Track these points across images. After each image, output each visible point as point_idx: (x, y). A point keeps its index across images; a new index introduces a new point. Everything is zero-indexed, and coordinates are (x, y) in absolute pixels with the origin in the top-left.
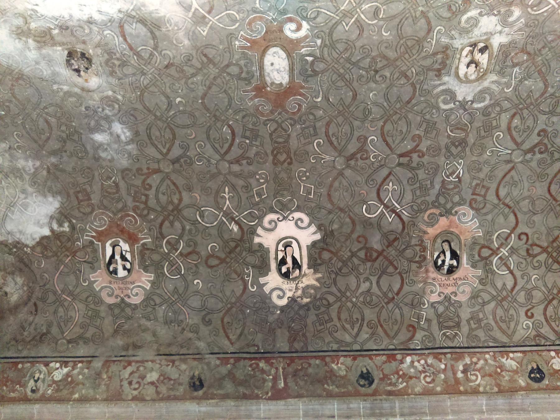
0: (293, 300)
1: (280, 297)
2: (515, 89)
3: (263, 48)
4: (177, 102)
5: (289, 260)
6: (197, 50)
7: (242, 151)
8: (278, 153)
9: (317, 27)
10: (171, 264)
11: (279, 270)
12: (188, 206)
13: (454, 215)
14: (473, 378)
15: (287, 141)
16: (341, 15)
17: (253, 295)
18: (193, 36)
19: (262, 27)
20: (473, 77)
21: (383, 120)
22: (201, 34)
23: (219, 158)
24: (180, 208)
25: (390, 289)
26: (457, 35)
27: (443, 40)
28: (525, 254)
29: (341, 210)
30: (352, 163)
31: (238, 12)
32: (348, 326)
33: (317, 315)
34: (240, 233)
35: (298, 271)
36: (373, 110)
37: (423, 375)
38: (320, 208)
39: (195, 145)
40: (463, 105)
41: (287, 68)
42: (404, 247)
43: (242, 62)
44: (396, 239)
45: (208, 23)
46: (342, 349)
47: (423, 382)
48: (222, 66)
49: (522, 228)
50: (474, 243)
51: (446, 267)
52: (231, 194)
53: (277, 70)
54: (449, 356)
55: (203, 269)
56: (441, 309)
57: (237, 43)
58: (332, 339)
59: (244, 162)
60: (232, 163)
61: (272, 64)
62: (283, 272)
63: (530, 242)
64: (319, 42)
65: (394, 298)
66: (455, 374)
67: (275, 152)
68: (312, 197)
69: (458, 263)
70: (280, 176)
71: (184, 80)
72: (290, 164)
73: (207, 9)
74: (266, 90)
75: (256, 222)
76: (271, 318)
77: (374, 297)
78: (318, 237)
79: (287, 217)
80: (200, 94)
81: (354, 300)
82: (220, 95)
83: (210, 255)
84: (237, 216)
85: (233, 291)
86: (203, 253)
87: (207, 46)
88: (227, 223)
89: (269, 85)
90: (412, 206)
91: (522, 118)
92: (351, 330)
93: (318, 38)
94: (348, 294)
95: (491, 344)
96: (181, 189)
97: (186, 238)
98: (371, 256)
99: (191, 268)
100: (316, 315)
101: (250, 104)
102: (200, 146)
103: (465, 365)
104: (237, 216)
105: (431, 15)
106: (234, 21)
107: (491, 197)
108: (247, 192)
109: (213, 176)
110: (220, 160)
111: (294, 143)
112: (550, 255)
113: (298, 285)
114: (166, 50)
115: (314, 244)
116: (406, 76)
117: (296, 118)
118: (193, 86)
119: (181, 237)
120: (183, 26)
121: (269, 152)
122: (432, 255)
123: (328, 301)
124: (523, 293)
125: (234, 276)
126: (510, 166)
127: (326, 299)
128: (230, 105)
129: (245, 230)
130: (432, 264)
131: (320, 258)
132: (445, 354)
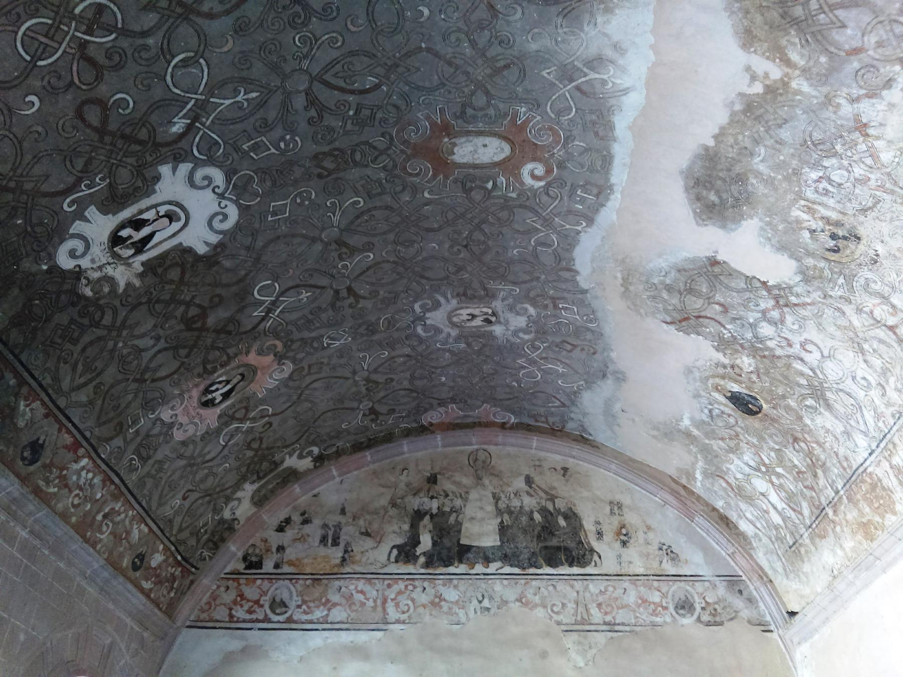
0: (78, 273)
1: (72, 254)
2: (439, 349)
3: (511, 137)
4: (421, 8)
5: (145, 231)
6: (518, 59)
7: (333, 108)
8: (334, 156)
9: (535, 195)
10: (52, 32)
11: (122, 226)
12: (201, 35)
13: (279, 364)
14: (104, 528)
15: (356, 164)
16: (547, 217)
17: (57, 212)
18: (542, 59)
19: (542, 141)
20: (455, 319)
21: (396, 260)
22: (545, 69)
23: (314, 74)
24: (191, 16)
25: (155, 370)
26: (506, 302)
27: (502, 293)
28: (248, 441)
29: (258, 260)
30: (334, 246)
31: (571, 120)
32: (80, 367)
33: (72, 321)
34: (170, 139)
35: (131, 252)
36: (411, 249)
37: (77, 492)
38: (253, 234)
39: (334, 32)
40: (421, 319)
41: (477, 162)
42: (221, 345)
43: (491, 112)
44: (229, 333)
45: (561, 82)
46: (50, 391)
47: (70, 500)
48: (489, 87)
49: (275, 421)
50: (248, 398)
51: (210, 397)
52: (246, 104)
53: (475, 151)
54: (113, 487)
55: (67, 101)
56: (156, 430)
57: (524, 109)
58: (53, 369)
59: (313, 113)
60: (307, 94)
61: (485, 146)
62: (119, 234)
63: (262, 435)
64: (514, 195)
65: (145, 381)
66: (98, 512)
67: (336, 153)
68: (270, 219)
69: (221, 402)
70: (296, 168)
71: (466, 29)
72: (320, 176)
73: (584, 88)
74: (444, 137)
75: (201, 157)
76: (27, 265)
77: (136, 362)
78: (202, 249)
79: (224, 198)
80: (439, 47)
81: (120, 345)
82: (436, 77)
83: (107, 105)
84: (203, 124)
85: (47, 177)
86: (103, 89)
87: (523, 73)
88: (185, 111)
89: (453, 140)
90: (282, 324)
91: (404, 363)
92: (77, 377)
93: (519, 195)
94: (125, 333)
95: (144, 504)
96: (237, 13)
97: (125, 43)
98: (195, 322)
99: (59, 78)
100: (72, 319)
101: (419, 115)
102: (333, 40)
103: (113, 509)
104: (203, 124)
105: (535, 283)
106: (559, 113)
107: (308, 380)
108: (255, 129)
109: (275, 68)
110: (311, 75)
111: (354, 173)
112: (253, 458)
113: (108, 266)
114: (523, 13)
115: (189, 250)
116: (458, 271)
117: (398, 172)
118: (453, 38)
119: (125, 32)
120: (561, 49)
121: (337, 144)
122: (218, 377)
123: (102, 318)
124: (206, 471)
125: (80, 163)
126: (349, 375)
127: (103, 314)
128: (418, 88)
129: (180, 145)
130: (208, 382)
131: (166, 270)
132: (113, 482)
